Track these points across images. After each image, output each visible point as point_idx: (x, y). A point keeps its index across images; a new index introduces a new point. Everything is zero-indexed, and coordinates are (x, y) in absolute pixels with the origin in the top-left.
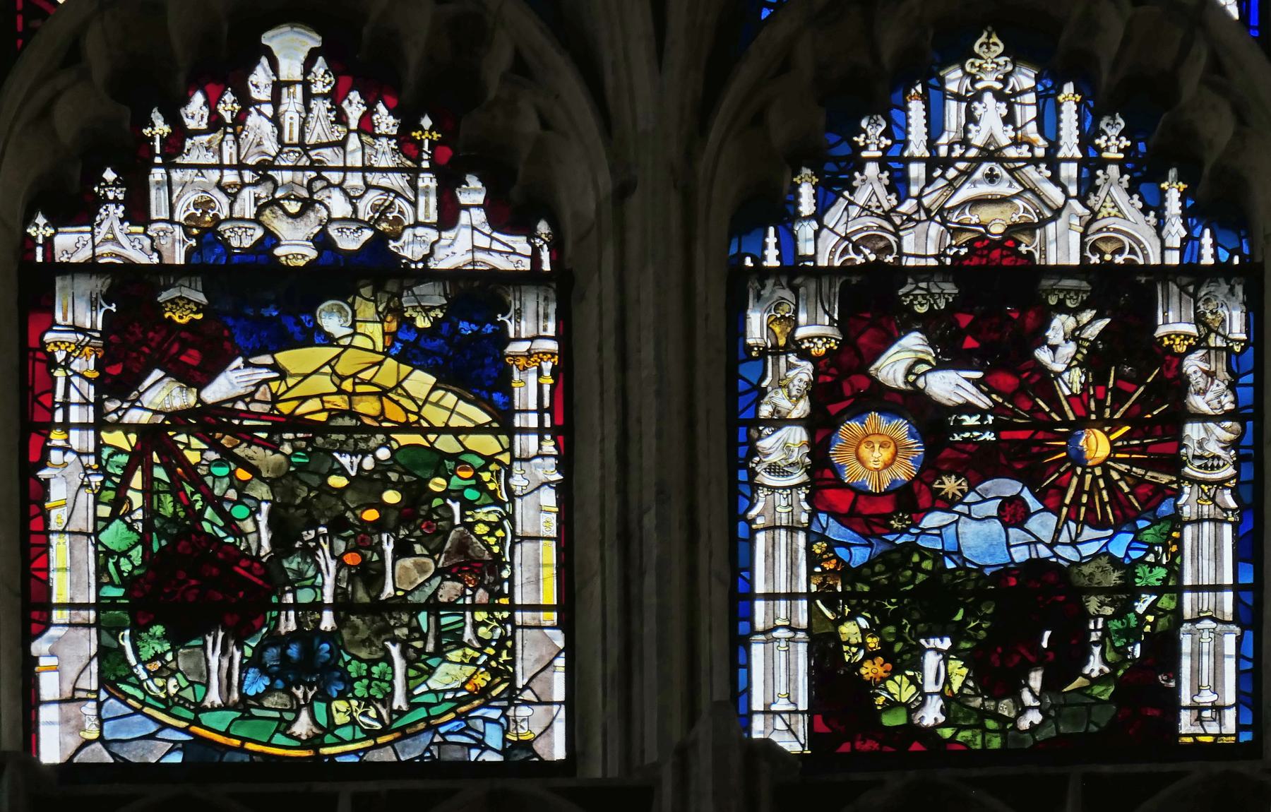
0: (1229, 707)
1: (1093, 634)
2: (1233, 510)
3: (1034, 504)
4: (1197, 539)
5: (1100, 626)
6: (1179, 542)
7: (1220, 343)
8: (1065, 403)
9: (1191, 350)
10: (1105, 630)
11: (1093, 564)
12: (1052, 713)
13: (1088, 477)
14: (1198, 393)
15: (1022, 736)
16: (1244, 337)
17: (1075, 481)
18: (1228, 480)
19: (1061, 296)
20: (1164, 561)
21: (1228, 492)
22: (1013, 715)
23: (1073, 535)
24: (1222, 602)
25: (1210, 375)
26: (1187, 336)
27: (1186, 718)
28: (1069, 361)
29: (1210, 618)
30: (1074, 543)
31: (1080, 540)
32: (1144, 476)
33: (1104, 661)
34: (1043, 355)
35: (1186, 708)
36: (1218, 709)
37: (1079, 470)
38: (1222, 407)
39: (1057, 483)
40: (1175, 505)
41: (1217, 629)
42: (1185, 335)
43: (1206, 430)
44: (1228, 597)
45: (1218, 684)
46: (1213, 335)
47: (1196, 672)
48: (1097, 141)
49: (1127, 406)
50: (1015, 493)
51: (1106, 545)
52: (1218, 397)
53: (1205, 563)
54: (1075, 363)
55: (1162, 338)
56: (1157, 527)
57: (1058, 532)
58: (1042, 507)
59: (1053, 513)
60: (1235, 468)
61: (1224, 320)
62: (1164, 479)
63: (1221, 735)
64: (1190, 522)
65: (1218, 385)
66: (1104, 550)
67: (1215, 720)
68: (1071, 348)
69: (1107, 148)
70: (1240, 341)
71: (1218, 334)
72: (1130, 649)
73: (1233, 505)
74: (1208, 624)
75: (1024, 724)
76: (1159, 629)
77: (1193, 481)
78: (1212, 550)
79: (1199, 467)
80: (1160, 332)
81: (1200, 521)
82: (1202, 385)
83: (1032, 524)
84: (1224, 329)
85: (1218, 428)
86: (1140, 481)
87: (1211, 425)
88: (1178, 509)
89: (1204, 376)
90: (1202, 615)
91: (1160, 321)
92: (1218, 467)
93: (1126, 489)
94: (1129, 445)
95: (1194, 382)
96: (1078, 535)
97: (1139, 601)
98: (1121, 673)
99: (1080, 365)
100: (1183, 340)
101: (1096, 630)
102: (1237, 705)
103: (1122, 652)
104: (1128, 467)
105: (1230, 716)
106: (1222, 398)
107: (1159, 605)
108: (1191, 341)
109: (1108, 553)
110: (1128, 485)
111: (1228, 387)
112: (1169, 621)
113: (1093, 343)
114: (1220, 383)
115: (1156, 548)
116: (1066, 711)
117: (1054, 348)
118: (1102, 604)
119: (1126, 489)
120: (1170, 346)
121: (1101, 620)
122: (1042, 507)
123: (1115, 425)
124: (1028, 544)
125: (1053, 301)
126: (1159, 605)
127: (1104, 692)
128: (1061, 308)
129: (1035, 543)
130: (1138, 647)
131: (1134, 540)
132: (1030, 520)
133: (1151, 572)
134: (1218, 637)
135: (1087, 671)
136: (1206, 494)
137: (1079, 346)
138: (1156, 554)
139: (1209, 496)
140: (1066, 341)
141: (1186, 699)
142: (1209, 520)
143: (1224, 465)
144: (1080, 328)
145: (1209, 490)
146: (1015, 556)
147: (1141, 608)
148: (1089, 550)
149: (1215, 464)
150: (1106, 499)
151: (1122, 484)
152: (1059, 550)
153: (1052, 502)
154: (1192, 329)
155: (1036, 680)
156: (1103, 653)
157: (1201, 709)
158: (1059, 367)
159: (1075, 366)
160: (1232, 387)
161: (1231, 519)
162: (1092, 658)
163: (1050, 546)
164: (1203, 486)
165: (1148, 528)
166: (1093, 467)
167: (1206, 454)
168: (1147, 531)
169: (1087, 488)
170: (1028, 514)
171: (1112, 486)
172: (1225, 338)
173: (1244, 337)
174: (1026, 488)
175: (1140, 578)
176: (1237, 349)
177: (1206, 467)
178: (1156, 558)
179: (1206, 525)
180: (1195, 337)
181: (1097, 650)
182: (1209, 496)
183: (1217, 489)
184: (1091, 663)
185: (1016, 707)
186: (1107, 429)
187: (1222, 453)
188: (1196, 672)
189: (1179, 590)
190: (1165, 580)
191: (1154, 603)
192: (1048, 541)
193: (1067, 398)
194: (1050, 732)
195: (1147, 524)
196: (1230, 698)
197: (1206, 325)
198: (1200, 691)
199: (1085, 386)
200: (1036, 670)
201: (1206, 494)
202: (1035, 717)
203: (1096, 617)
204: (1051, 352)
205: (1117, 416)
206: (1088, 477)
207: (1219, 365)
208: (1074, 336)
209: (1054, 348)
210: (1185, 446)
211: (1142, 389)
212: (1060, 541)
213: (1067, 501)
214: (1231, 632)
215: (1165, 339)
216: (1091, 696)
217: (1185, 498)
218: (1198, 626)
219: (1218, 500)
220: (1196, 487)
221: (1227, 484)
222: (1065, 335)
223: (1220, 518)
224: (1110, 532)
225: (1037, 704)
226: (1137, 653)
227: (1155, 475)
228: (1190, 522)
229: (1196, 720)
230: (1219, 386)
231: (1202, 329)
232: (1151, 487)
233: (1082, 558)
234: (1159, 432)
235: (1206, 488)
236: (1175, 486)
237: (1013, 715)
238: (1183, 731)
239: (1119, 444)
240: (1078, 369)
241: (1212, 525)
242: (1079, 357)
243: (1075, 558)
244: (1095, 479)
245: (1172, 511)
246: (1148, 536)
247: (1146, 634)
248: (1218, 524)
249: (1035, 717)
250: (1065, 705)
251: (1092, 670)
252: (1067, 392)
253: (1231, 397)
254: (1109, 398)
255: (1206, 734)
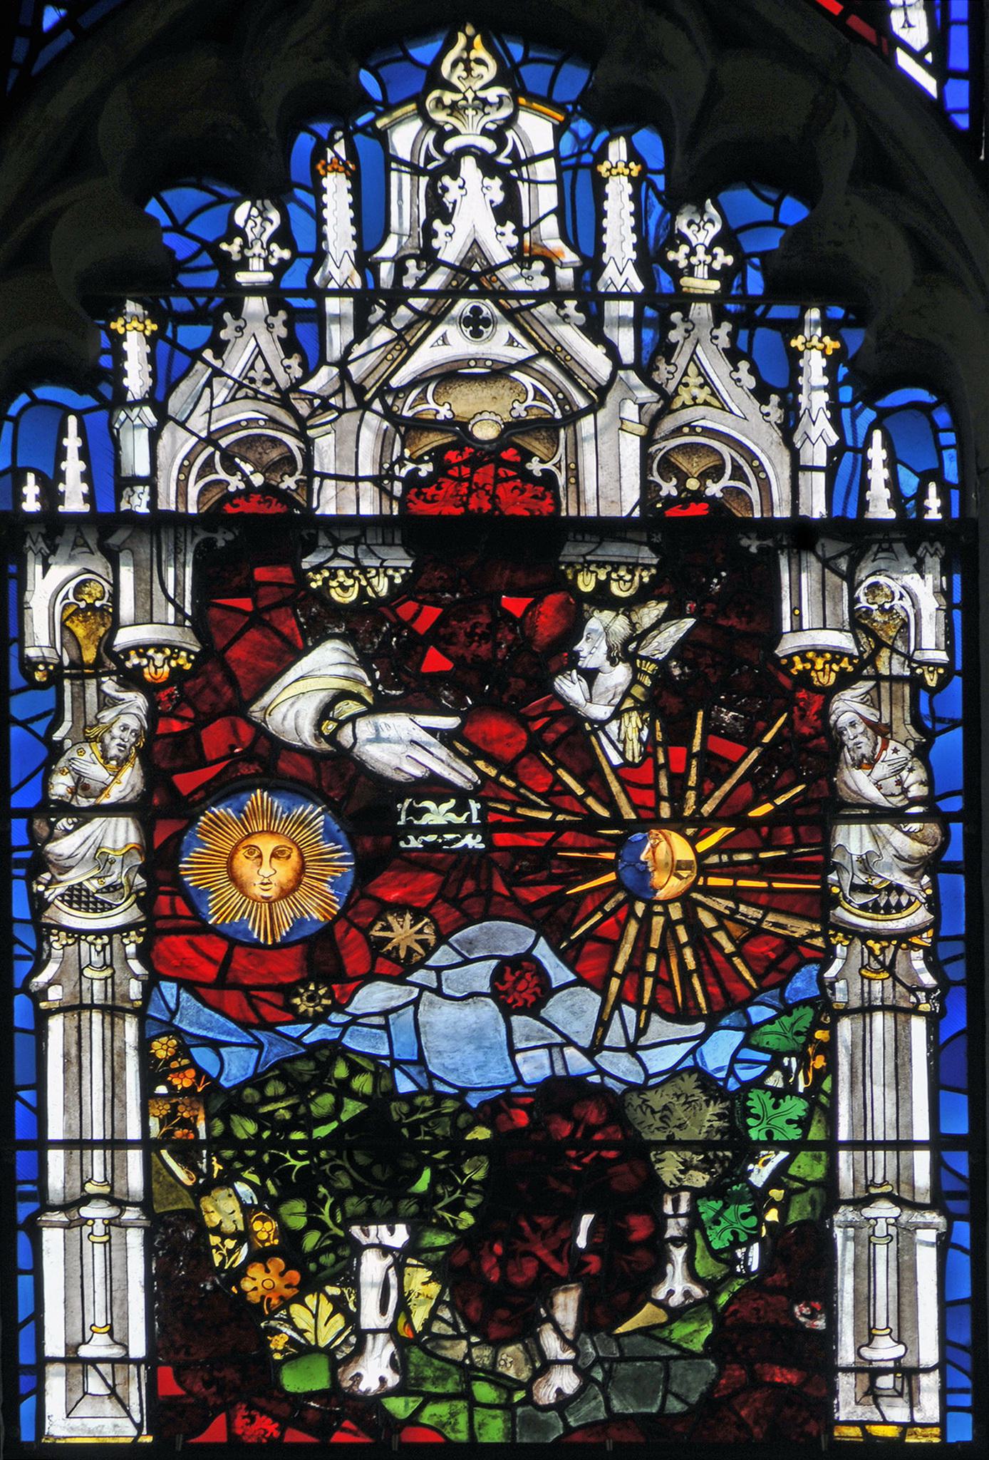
0: (927, 1371)
1: (671, 1222)
2: (929, 992)
3: (559, 973)
4: (863, 1042)
5: (684, 1208)
6: (829, 1049)
7: (899, 668)
8: (611, 778)
9: (845, 681)
10: (694, 1215)
11: (669, 1089)
12: (598, 1375)
13: (658, 922)
14: (859, 765)
15: (542, 1416)
16: (942, 656)
17: (633, 928)
18: (919, 932)
19: (603, 577)
20: (801, 1087)
21: (917, 955)
22: (525, 1375)
23: (631, 1032)
24: (911, 1166)
25: (881, 731)
26: (837, 655)
27: (846, 1385)
28: (617, 700)
29: (889, 1197)
30: (632, 1048)
31: (643, 1041)
32: (760, 921)
33: (693, 1275)
34: (571, 688)
35: (847, 1370)
36: (908, 1373)
37: (640, 908)
38: (905, 791)
39: (599, 932)
40: (820, 979)
41: (903, 1219)
42: (833, 653)
43: (875, 836)
44: (922, 1161)
45: (907, 1325)
46: (885, 653)
47: (865, 1301)
48: (671, 256)
49: (727, 787)
50: (522, 950)
51: (692, 1052)
52: (898, 772)
53: (878, 1090)
54: (629, 703)
55: (790, 657)
56: (786, 1020)
57: (603, 1024)
58: (572, 977)
59: (594, 989)
60: (930, 910)
61: (905, 625)
62: (800, 928)
63: (913, 1424)
64: (847, 1012)
65: (895, 751)
66: (689, 1062)
67: (900, 1395)
68: (621, 674)
69: (691, 270)
70: (937, 665)
71: (894, 650)
72: (740, 1253)
73: (928, 979)
74: (884, 1210)
75: (546, 1394)
76: (794, 1217)
77: (853, 933)
78: (890, 1067)
79: (863, 907)
80: (789, 644)
81: (867, 1010)
82: (866, 749)
83: (555, 1009)
84: (907, 642)
85: (897, 833)
86: (756, 931)
87: (885, 828)
88: (825, 987)
89: (870, 732)
90: (873, 1191)
91: (786, 626)
92: (899, 908)
93: (729, 948)
94: (732, 863)
95: (850, 744)
96: (641, 1032)
97: (756, 1162)
98: (723, 1299)
99: (640, 707)
100: (830, 662)
101: (676, 1215)
102: (942, 1366)
103: (726, 1257)
104: (731, 905)
105: (929, 1384)
106: (904, 773)
107: (793, 1170)
108: (845, 663)
109: (696, 1069)
110: (731, 938)
111: (914, 754)
112: (813, 1202)
113: (663, 665)
114: (899, 747)
115: (786, 1061)
116: (623, 1368)
117: (590, 676)
118: (687, 1167)
119: (729, 948)
120: (805, 674)
121: (685, 1197)
122: (572, 977)
123: (703, 825)
124: (549, 1047)
125: (586, 583)
126: (793, 1170)
127: (697, 1334)
128: (602, 598)
129: (561, 1046)
130: (755, 1249)
131: (745, 1044)
132: (552, 1001)
133: (776, 1106)
134: (904, 1236)
135: (660, 1294)
136: (876, 957)
137: (636, 671)
138: (787, 1072)
139: (882, 964)
140: (613, 662)
141: (846, 1355)
142: (884, 1008)
143: (910, 904)
144: (639, 636)
145: (883, 950)
146: (523, 1069)
147: (759, 1175)
148: (661, 1060)
149: (893, 901)
150: (691, 964)
151: (721, 937)
152: (604, 1059)
153: (591, 966)
154: (844, 641)
155: (567, 1307)
156: (690, 1260)
157: (876, 1373)
158: (600, 711)
159: (628, 710)
160: (921, 753)
161: (925, 1007)
162: (669, 1268)
163: (590, 1052)
164: (870, 943)
165: (770, 1021)
166: (665, 903)
167: (876, 882)
168: (768, 1028)
169: (655, 943)
170: (546, 991)
171: (700, 938)
172: (909, 658)
173: (942, 656)
174: (542, 940)
175: (757, 1117)
176: (932, 681)
177: (875, 908)
178: (786, 1079)
179: (878, 1016)
180: (851, 657)
181: (679, 1254)
182: (882, 964)
183: (897, 947)
184: (668, 1278)
185: (530, 1360)
186: (690, 831)
187: (905, 881)
188: (865, 1301)
189: (831, 1146)
190: (804, 1124)
191: (783, 1166)
192: (585, 1042)
193: (615, 769)
194: (593, 1410)
195: (770, 1013)
196: (929, 1352)
197: (870, 633)
198: (871, 1337)
199: (649, 748)
200: (566, 1290)
201: (876, 957)
202: (566, 1380)
203: (676, 1191)
204: (584, 684)
205: (707, 809)
206: (658, 922)
207: (898, 713)
208: (625, 653)
209: (590, 676)
210: (836, 867)
211: (754, 755)
212: (607, 1043)
213: (619, 967)
214: (927, 1226)
215: (797, 659)
216: (668, 1342)
217: (837, 966)
218: (868, 1212)
219: (900, 969)
220: (858, 943)
221: (915, 940)
222: (610, 649)
223: (903, 1004)
224: (700, 1027)
225: (570, 1355)
226: (754, 1264)
227: (782, 920)
228: (847, 1012)
229: (866, 1394)
230: (897, 753)
231: (864, 640)
232: (777, 942)
233: (649, 1076)
234: (789, 839)
235: (877, 947)
236: (818, 942)
237: (525, 1375)
238: (842, 1415)
239: (714, 859)
240: (634, 714)
241: (890, 1017)
242: (637, 691)
243: (637, 1077)
244: (670, 925)
245: (814, 991)
246: (772, 1038)
247: (770, 1225)
248: (901, 1017)
249: (566, 1380)
250: (623, 1359)
251: (671, 1293)
252: (616, 760)
253: (920, 774)
254: (694, 771)
255: (885, 1423)
